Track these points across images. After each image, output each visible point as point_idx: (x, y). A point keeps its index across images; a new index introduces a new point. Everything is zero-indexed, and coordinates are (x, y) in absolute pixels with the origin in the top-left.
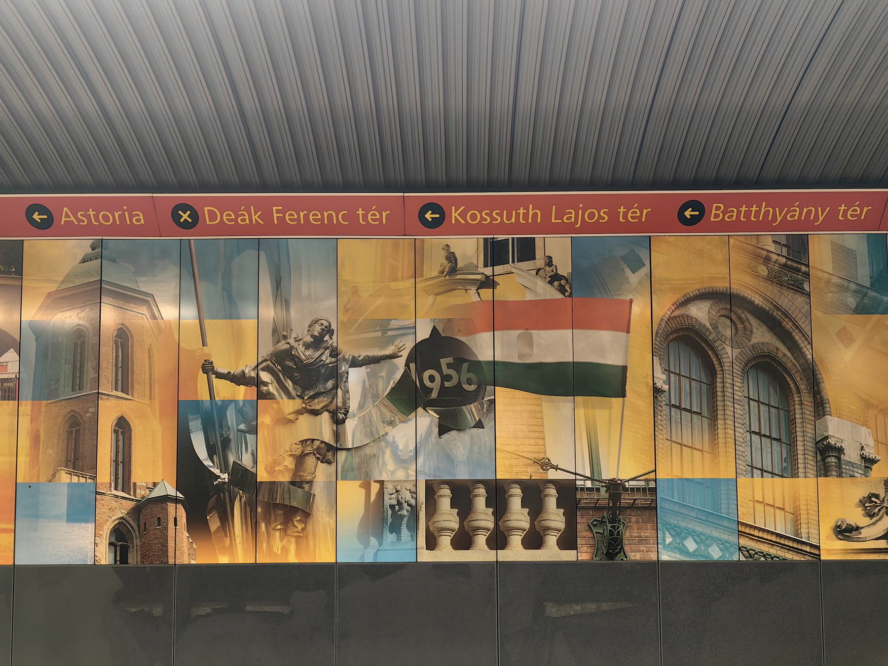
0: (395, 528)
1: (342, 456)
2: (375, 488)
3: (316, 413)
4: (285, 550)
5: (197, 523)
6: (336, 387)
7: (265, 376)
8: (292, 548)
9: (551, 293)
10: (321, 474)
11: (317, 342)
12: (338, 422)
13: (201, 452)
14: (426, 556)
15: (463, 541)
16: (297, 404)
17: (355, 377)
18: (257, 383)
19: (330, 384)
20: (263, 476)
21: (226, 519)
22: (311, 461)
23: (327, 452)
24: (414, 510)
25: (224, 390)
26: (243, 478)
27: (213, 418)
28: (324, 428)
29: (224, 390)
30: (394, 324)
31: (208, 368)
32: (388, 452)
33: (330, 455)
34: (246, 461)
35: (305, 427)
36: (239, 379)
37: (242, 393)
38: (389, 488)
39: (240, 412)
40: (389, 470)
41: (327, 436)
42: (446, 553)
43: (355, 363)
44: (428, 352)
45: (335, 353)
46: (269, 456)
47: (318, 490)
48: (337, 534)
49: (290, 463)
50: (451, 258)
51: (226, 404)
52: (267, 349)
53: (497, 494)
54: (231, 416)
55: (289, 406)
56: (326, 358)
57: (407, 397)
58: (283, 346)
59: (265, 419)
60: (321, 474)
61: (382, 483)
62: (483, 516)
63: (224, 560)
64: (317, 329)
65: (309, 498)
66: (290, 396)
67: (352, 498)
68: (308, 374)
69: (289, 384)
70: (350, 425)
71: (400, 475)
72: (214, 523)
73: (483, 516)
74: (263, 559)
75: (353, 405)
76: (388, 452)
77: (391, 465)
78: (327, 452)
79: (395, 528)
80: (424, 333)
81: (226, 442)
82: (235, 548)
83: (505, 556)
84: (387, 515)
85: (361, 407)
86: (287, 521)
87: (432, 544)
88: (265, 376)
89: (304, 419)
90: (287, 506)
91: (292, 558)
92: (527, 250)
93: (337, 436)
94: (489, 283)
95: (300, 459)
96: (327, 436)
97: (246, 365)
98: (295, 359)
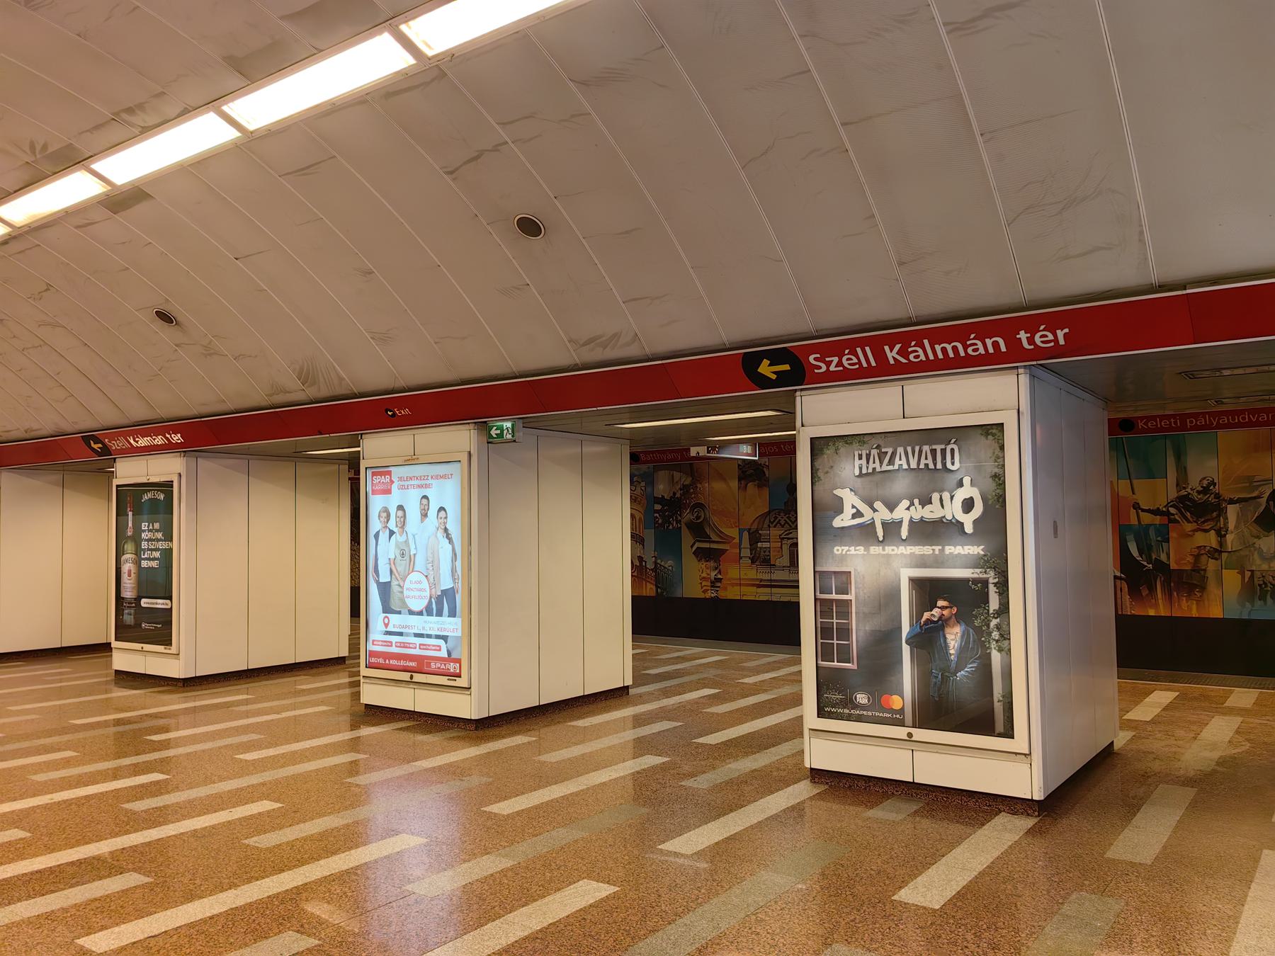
0: (1262, 598)
1: (1224, 556)
2: (1248, 574)
3: (1206, 531)
4: (1190, 609)
6: (1219, 516)
7: (1172, 510)
8: (1194, 607)
10: (1212, 565)
11: (1205, 490)
13: (1135, 552)
16: (1194, 526)
17: (1232, 511)
18: (1168, 514)
19: (1215, 514)
20: (1173, 566)
21: (1152, 589)
22: (1204, 558)
23: (1215, 553)
25: (1147, 518)
26: (1162, 567)
28: (1211, 540)
29: (1147, 518)
30: (1257, 478)
31: (1136, 506)
32: (1256, 555)
33: (1216, 555)
34: (1163, 557)
36: (1156, 512)
37: (1157, 520)
38: (1258, 574)
41: (1214, 544)
43: (1232, 502)
45: (1217, 496)
46: (1176, 555)
47: (1210, 574)
48: (1223, 600)
49: (1190, 559)
51: (1149, 526)
52: (1173, 494)
54: (1152, 533)
55: (1189, 527)
56: (1212, 499)
58: (1183, 493)
59: (1173, 535)
60: (1212, 565)
61: (1252, 571)
63: (1152, 613)
64: (1205, 483)
65: (1204, 578)
66: (1189, 522)
67: (1232, 579)
68: (1203, 508)
69: (1188, 515)
70: (1229, 538)
71: (1265, 567)
72: (1145, 592)
74: (1177, 613)
75: (1231, 525)
76: (1256, 555)
77: (1258, 562)
78: (1215, 553)
81: (1150, 547)
84: (1256, 588)
85: (1236, 527)
88: (1172, 510)
89: (1199, 535)
90: (1190, 582)
91: (1194, 613)
93: (1221, 544)
95: (1197, 557)
96: (1214, 544)
97: (1161, 503)
98: (1190, 500)
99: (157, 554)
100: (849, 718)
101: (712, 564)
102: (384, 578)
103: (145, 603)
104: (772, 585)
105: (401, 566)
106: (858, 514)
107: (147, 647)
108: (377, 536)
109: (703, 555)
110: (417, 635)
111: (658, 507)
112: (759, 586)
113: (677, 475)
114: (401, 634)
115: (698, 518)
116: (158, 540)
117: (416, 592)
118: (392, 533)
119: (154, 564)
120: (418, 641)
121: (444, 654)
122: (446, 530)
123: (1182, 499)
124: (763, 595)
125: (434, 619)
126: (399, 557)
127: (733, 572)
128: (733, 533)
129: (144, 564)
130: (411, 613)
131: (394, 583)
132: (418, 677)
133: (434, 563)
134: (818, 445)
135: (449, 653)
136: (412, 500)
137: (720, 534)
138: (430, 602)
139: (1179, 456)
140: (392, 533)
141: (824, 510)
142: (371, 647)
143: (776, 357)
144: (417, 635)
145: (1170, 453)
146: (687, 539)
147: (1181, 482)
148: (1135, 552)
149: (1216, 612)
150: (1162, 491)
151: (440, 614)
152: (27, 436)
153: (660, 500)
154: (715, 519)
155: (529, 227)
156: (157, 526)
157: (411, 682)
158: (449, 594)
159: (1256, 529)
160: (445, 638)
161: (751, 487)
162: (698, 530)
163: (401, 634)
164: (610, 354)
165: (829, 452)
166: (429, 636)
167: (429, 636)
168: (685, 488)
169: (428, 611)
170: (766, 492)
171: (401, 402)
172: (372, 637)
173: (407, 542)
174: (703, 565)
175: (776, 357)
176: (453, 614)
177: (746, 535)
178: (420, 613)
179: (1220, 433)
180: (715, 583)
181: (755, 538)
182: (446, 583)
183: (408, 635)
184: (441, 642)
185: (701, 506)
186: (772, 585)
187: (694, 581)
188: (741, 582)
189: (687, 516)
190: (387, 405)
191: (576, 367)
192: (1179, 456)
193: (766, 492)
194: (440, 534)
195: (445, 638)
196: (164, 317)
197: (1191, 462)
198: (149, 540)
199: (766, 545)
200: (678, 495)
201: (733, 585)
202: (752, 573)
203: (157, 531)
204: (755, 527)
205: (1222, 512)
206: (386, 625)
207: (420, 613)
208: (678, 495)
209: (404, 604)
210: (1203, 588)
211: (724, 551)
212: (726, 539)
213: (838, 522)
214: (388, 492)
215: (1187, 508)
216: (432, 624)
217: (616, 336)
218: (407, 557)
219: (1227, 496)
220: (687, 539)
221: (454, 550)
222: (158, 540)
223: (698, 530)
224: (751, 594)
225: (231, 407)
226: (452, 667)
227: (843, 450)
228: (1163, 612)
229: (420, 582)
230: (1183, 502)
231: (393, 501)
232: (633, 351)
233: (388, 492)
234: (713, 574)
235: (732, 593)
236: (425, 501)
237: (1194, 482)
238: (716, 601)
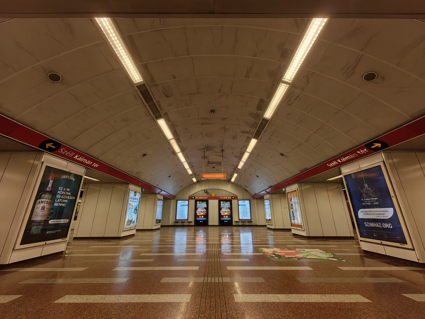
99: (67, 201)
107: (48, 242)
116: (67, 195)
119: (63, 205)
156: (68, 190)
190: (140, 182)
196: (145, 155)
198: (61, 195)
203: (68, 192)
222: (67, 195)
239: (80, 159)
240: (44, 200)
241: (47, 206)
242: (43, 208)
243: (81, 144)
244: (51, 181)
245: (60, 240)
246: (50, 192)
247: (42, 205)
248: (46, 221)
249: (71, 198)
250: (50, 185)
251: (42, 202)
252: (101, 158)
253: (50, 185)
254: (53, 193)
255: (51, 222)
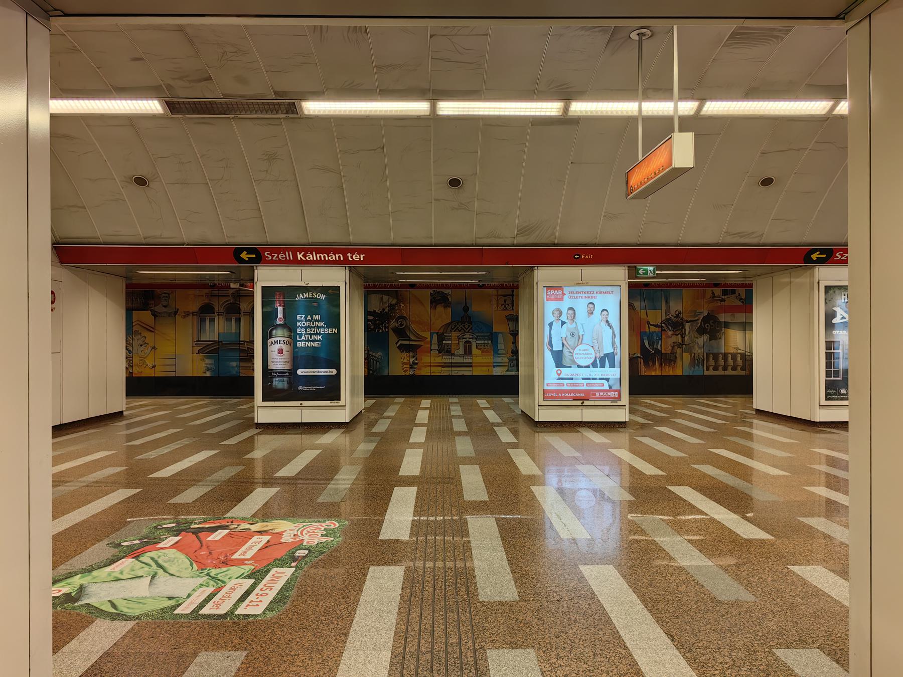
0: (698, 365)
5: (646, 364)
9: (740, 303)
10: (679, 351)
11: (677, 316)
12: (683, 338)
13: (647, 345)
14: (706, 373)
15: (716, 368)
17: (687, 325)
18: (662, 327)
20: (663, 351)
21: (654, 363)
23: (680, 345)
24: (703, 360)
25: (653, 329)
26: (658, 352)
27: (650, 336)
31: (648, 323)
34: (659, 347)
35: (674, 339)
37: (657, 329)
39: (657, 335)
40: (697, 350)
42: (711, 372)
43: (687, 322)
44: (706, 319)
45: (682, 319)
46: (665, 345)
47: (678, 355)
48: (682, 367)
50: (713, 293)
52: (664, 318)
53: (725, 356)
54: (654, 335)
55: (670, 333)
57: (701, 331)
59: (664, 337)
60: (679, 351)
62: (721, 362)
65: (676, 357)
67: (686, 357)
68: (676, 324)
70: (686, 338)
73: (721, 362)
75: (687, 333)
78: (680, 345)
79: (698, 365)
80: (705, 314)
81: (653, 343)
82: (656, 372)
83: (727, 373)
84: (695, 362)
86: (670, 364)
87: (708, 369)
90: (669, 359)
92: (733, 292)
94: (723, 300)
95: (673, 347)
97: (659, 322)
99: (320, 337)
100: (837, 399)
101: (411, 354)
102: (557, 347)
103: (300, 372)
104: (451, 365)
105: (571, 341)
106: (843, 318)
107: (305, 403)
108: (551, 325)
109: (402, 348)
110: (583, 379)
111: (371, 318)
112: (443, 367)
113: (385, 298)
114: (572, 379)
115: (401, 325)
117: (584, 354)
118: (563, 323)
119: (316, 344)
120: (585, 382)
121: (606, 387)
122: (607, 321)
123: (667, 320)
124: (446, 372)
125: (599, 369)
126: (569, 336)
127: (426, 359)
128: (427, 335)
129: (300, 344)
130: (579, 366)
131: (566, 351)
132: (586, 403)
133: (599, 340)
134: (828, 289)
135: (610, 387)
136: (581, 306)
137: (417, 335)
138: (595, 361)
139: (667, 301)
140: (563, 323)
141: (830, 316)
142: (546, 388)
143: (822, 251)
144: (583, 379)
145: (663, 298)
146: (393, 338)
147: (668, 312)
148: (647, 345)
149: (679, 373)
150: (657, 316)
151: (603, 366)
152: (144, 241)
153: (373, 313)
154: (413, 326)
155: (767, 182)
156: (317, 317)
157: (582, 405)
158: (610, 357)
159: (696, 334)
160: (607, 380)
161: (440, 309)
162: (401, 333)
163: (572, 379)
164: (742, 241)
165: (831, 292)
166: (595, 379)
167: (595, 379)
168: (392, 307)
169: (594, 365)
170: (449, 310)
171: (587, 252)
172: (546, 382)
173: (576, 328)
174: (404, 355)
175: (822, 251)
176: (612, 365)
177: (435, 337)
178: (588, 367)
179: (684, 290)
180: (412, 366)
181: (441, 338)
182: (608, 349)
183: (577, 379)
184: (605, 382)
185: (404, 318)
186: (451, 365)
187: (398, 365)
188: (482, 363)
189: (393, 324)
190: (579, 252)
191: (717, 245)
192: (667, 301)
193: (449, 310)
194: (603, 324)
195: (607, 380)
197: (672, 304)
198: (306, 328)
199: (449, 342)
200: (386, 310)
201: (426, 366)
202: (439, 359)
203: (318, 321)
204: (442, 331)
205: (684, 326)
206: (559, 375)
207: (588, 367)
208: (386, 310)
209: (574, 362)
210: (675, 362)
211: (420, 346)
212: (423, 339)
213: (834, 321)
214: (562, 299)
215: (670, 324)
216: (598, 372)
217: (753, 233)
218: (576, 336)
219: (686, 319)
220: (393, 338)
221: (613, 332)
222: (318, 327)
223: (401, 333)
224: (437, 371)
225: (434, 241)
226: (612, 394)
227: (837, 291)
228: (658, 373)
229: (587, 350)
230: (667, 321)
231: (565, 305)
232: (755, 241)
233: (562, 299)
234: (411, 360)
235: (425, 372)
236: (591, 306)
237: (673, 313)
238: (413, 377)
239: (310, 257)
240: (278, 339)
241: (285, 348)
242: (280, 351)
243: (284, 232)
244: (280, 309)
245: (328, 403)
246: (283, 326)
247: (277, 346)
248: (292, 372)
249: (330, 331)
250: (280, 315)
251: (276, 342)
252: (352, 239)
253: (280, 315)
254: (290, 327)
255: (300, 372)
